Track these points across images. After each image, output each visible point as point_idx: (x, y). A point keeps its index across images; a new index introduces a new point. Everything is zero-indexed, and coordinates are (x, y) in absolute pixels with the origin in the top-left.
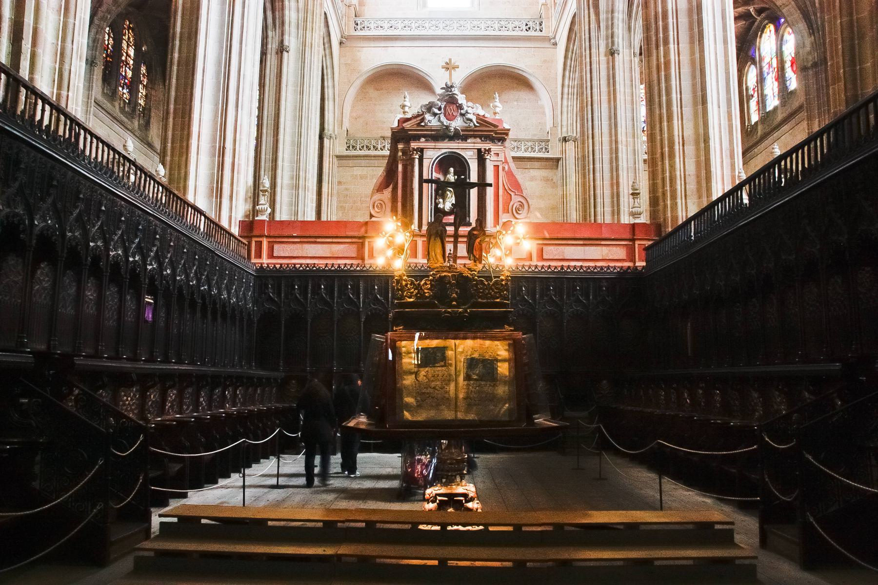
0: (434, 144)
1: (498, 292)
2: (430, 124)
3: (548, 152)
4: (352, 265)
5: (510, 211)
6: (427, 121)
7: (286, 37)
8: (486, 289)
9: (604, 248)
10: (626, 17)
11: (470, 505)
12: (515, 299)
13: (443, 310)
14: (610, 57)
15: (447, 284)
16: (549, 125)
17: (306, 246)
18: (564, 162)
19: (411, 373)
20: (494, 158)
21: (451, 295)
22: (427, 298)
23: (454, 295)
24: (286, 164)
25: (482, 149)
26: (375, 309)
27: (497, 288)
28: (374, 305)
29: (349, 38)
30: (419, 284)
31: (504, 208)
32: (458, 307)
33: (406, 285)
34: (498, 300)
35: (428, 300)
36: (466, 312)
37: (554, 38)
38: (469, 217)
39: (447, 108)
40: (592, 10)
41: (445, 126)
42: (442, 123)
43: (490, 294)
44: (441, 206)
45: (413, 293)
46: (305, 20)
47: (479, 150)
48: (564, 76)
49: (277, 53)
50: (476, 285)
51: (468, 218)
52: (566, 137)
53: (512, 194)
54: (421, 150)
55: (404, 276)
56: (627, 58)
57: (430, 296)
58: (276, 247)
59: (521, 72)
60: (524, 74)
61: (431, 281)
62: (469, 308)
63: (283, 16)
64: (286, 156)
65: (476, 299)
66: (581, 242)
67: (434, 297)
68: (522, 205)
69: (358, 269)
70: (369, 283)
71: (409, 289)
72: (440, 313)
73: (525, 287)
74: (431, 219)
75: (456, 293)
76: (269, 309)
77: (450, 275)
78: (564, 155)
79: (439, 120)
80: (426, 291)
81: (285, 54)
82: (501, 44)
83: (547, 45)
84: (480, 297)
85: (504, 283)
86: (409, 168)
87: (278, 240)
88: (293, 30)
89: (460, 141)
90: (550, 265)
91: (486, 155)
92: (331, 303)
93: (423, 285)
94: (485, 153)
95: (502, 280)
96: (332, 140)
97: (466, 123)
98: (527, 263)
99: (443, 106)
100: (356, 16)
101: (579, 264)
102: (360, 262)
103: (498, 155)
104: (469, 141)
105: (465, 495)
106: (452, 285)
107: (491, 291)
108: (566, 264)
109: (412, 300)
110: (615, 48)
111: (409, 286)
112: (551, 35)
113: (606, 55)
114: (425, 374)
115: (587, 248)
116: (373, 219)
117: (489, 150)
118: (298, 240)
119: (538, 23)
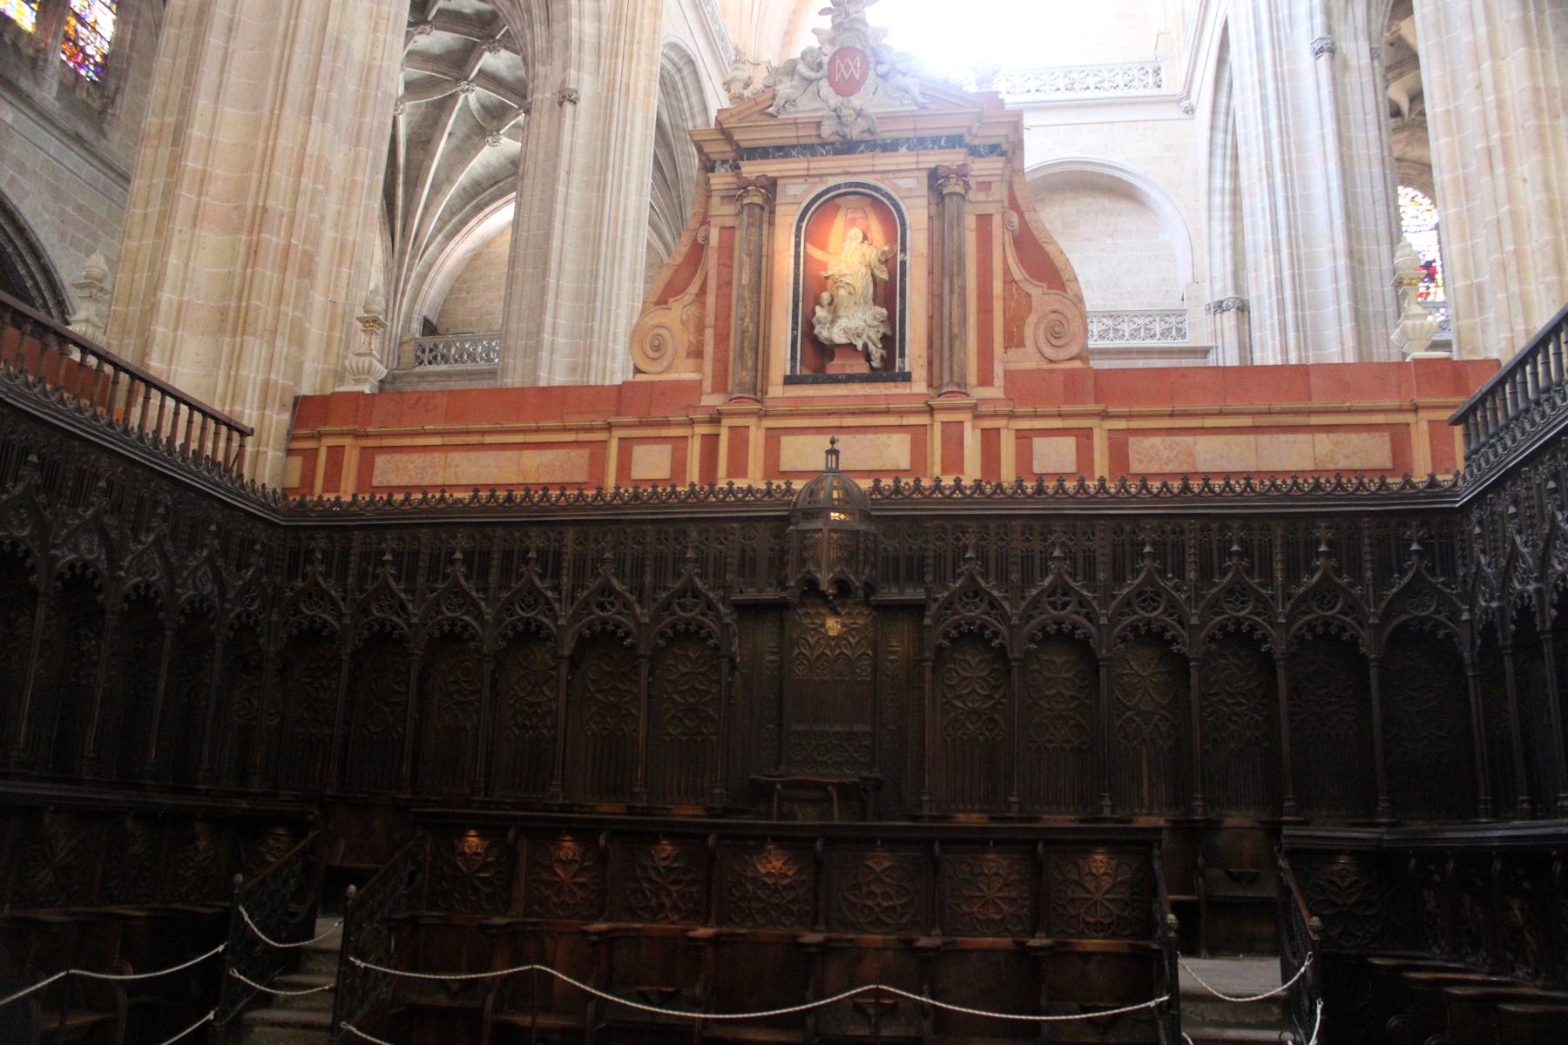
0: (805, 165)
3: (1184, 336)
7: (573, 72)
9: (1321, 437)
16: (1184, 276)
17: (456, 457)
18: (1220, 355)
24: (561, 340)
26: (604, 622)
37: (1188, 96)
38: (902, 355)
39: (838, 61)
44: (823, 333)
46: (615, 38)
48: (1210, 170)
49: (552, 107)
52: (1222, 302)
54: (770, 186)
58: (381, 460)
59: (1117, 174)
60: (1125, 177)
63: (568, 28)
64: (562, 322)
74: (793, 367)
76: (312, 620)
78: (1220, 341)
81: (568, 107)
82: (1071, 117)
83: (1174, 112)
87: (387, 442)
88: (588, 59)
99: (826, 60)
104: (903, 150)
115: (1265, 439)
117: (962, 173)
118: (437, 441)
119: (1151, 71)
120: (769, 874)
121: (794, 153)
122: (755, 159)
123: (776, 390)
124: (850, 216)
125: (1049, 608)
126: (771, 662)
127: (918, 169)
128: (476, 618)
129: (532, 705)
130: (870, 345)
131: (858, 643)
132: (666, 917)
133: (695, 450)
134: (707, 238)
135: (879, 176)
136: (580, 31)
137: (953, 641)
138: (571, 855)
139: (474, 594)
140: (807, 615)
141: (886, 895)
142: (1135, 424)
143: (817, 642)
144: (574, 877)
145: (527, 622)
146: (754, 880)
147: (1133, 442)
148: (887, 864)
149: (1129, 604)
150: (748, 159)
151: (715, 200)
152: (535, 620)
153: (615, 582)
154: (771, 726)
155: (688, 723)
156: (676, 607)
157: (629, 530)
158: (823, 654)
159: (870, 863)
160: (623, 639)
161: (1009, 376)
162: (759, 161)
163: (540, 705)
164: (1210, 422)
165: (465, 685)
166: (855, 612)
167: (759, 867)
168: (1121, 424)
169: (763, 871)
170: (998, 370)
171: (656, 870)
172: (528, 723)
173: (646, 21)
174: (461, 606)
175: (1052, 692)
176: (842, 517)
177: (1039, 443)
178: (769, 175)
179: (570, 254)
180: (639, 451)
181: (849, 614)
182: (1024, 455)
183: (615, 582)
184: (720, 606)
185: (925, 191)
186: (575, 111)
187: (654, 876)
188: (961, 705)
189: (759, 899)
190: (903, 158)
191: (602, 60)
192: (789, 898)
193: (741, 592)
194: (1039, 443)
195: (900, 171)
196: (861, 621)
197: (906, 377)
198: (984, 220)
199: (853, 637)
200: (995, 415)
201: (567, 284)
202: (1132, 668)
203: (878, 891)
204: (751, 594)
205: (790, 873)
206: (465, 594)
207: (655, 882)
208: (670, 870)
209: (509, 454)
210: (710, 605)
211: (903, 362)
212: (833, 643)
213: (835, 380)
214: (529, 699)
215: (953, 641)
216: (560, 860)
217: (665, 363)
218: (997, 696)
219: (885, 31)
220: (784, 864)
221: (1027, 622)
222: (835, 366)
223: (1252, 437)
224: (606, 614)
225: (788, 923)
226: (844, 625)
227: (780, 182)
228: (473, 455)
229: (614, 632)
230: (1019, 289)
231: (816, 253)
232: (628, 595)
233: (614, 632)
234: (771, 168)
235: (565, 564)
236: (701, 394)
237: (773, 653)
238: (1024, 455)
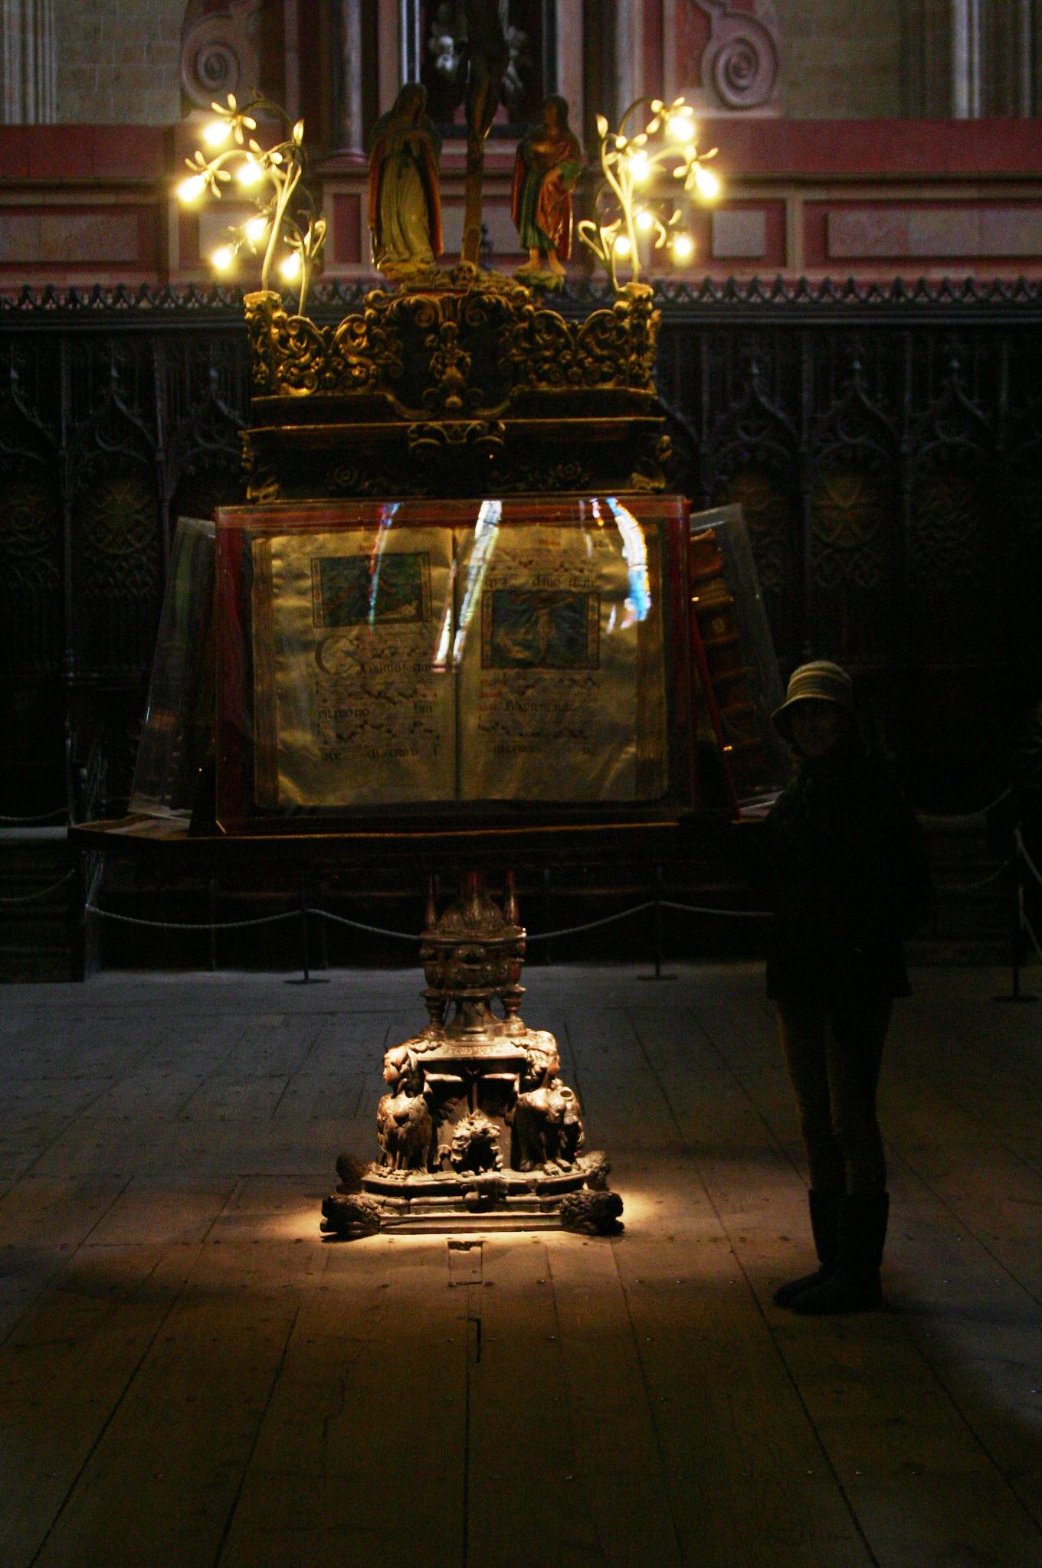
1: (610, 358)
4: (120, 292)
5: (706, 80)
8: (567, 346)
11: (538, 1098)
13: (414, 425)
15: (428, 331)
19: (306, 646)
21: (443, 373)
22: (358, 382)
23: (453, 372)
27: (602, 344)
30: (328, 336)
32: (467, 412)
33: (284, 340)
34: (609, 386)
35: (360, 391)
36: (493, 426)
43: (580, 364)
45: (307, 366)
50: (529, 335)
53: (715, 13)
55: (276, 307)
57: (368, 376)
61: (371, 322)
62: (503, 416)
65: (529, 382)
67: (385, 378)
68: (750, 58)
69: (144, 304)
71: (294, 356)
72: (402, 435)
73: (759, 361)
75: (460, 365)
77: (436, 299)
80: (354, 360)
84: (543, 377)
85: (626, 323)
90: (851, 282)
93: (344, 338)
95: (621, 314)
98: (767, 275)
101: (958, 274)
102: (152, 279)
105: (519, 1065)
106: (443, 337)
107: (582, 355)
108: (911, 275)
109: (304, 392)
111: (291, 342)
114: (351, 648)
115: (991, 215)
125: (742, 434)
142: (837, 194)
147: (834, 215)
153: (221, 404)
164: (927, 194)
165: (21, 536)
168: (819, 195)
209: (24, 220)
214: (111, 551)
223: (975, 214)
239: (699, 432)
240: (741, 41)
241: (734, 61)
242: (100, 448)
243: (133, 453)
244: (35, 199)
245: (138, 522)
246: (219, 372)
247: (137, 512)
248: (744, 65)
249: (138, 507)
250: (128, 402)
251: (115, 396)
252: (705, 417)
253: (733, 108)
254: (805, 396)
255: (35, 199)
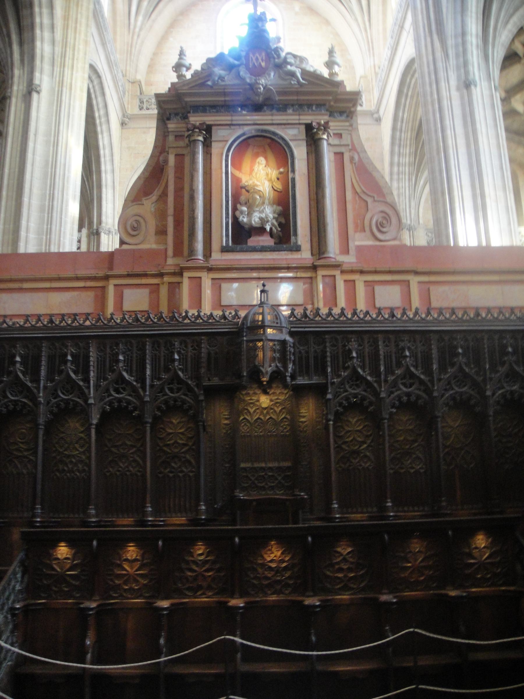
2: (223, 83)
5: (367, 229)
6: (216, 78)
10: (480, 42)
12: (393, 373)
14: (465, 91)
20: (334, 141)
25: (314, 124)
26: (120, 400)
28: (118, 392)
29: (132, 118)
31: (356, 226)
38: (296, 234)
40: (435, 37)
41: (249, 84)
42: (243, 79)
44: (244, 219)
47: (309, 127)
51: (293, 238)
53: (370, 200)
54: (208, 129)
56: (486, 92)
64: (33, 225)
66: (496, 278)
69: (88, 323)
70: (108, 350)
73: (409, 349)
74: (227, 241)
79: (238, 76)
86: (187, 160)
88: (47, 67)
89: (274, 111)
91: (320, 133)
92: (35, 391)
94: (318, 129)
96: (111, 236)
97: (283, 79)
100: (141, 94)
103: (340, 136)
104: (290, 111)
110: (471, 77)
112: (373, 108)
113: (458, 89)
116: (125, 247)
120: (272, 561)
121: (222, 110)
122: (197, 112)
123: (217, 256)
124: (255, 150)
125: (402, 387)
126: (225, 424)
127: (300, 124)
128: (31, 400)
129: (68, 456)
130: (273, 228)
131: (281, 411)
132: (203, 594)
133: (164, 291)
134: (166, 161)
135: (276, 127)
136: (42, 50)
137: (344, 407)
138: (135, 555)
139: (29, 384)
140: (248, 394)
141: (350, 570)
142: (433, 278)
143: (255, 411)
144: (137, 570)
145: (67, 402)
146: (263, 565)
147: (432, 288)
148: (349, 550)
149: (449, 383)
150: (193, 112)
151: (171, 138)
152: (73, 401)
153: (125, 374)
154: (227, 465)
155: (173, 465)
156: (167, 391)
157: (133, 341)
158: (259, 418)
159: (339, 549)
160: (132, 412)
161: (359, 249)
162: (200, 114)
163: (73, 456)
165: (21, 445)
166: (278, 391)
167: (265, 556)
169: (269, 559)
170: (352, 245)
171: (195, 562)
172: (66, 468)
173: (81, 47)
174: (21, 392)
175: (402, 438)
176: (275, 331)
177: (378, 289)
178: (208, 123)
179: (37, 184)
180: (127, 293)
181: (273, 393)
182: (371, 296)
183: (125, 374)
184: (196, 389)
185: (304, 136)
186: (39, 98)
187: (194, 567)
188: (347, 448)
189: (267, 578)
190: (291, 117)
191: (55, 68)
192: (287, 575)
193: (209, 380)
194: (378, 289)
195: (289, 124)
196: (282, 397)
197: (298, 249)
198: (340, 156)
199: (278, 407)
200: (352, 272)
201: (35, 202)
202: (447, 423)
203: (345, 567)
204: (216, 381)
205: (287, 559)
206: (23, 385)
207: (195, 571)
208: (205, 562)
209: (41, 295)
210: (190, 389)
211: (296, 239)
212: (265, 412)
213: (254, 250)
214: (66, 452)
215: (344, 407)
216: (127, 560)
217: (140, 238)
218: (369, 441)
219: (278, 39)
220: (282, 553)
221: (389, 396)
222: (254, 241)
224: (121, 396)
225: (287, 592)
226: (271, 400)
227: (214, 128)
228: (16, 296)
229: (127, 407)
230: (360, 197)
231: (237, 173)
232: (135, 383)
233: (127, 407)
234: (209, 119)
235: (92, 363)
236: (166, 257)
237: (226, 419)
238: (371, 296)
239: (380, 387)
240: (382, 212)
241: (380, 220)
242: (60, 396)
243: (78, 400)
244: (47, 285)
245: (82, 438)
246: (124, 357)
247: (82, 432)
248: (384, 222)
249: (82, 429)
250: (75, 372)
251: (69, 370)
252: (383, 377)
253: (380, 241)
254: (435, 367)
255: (47, 285)
